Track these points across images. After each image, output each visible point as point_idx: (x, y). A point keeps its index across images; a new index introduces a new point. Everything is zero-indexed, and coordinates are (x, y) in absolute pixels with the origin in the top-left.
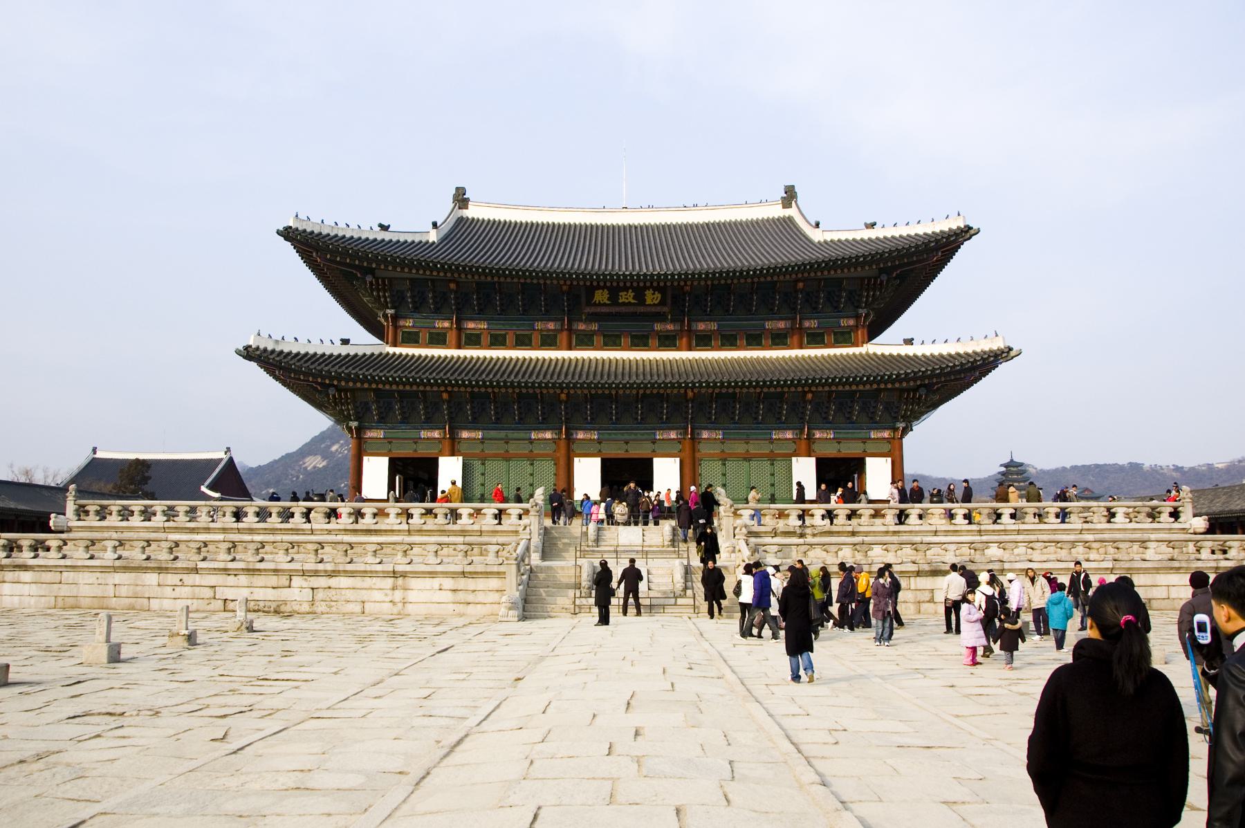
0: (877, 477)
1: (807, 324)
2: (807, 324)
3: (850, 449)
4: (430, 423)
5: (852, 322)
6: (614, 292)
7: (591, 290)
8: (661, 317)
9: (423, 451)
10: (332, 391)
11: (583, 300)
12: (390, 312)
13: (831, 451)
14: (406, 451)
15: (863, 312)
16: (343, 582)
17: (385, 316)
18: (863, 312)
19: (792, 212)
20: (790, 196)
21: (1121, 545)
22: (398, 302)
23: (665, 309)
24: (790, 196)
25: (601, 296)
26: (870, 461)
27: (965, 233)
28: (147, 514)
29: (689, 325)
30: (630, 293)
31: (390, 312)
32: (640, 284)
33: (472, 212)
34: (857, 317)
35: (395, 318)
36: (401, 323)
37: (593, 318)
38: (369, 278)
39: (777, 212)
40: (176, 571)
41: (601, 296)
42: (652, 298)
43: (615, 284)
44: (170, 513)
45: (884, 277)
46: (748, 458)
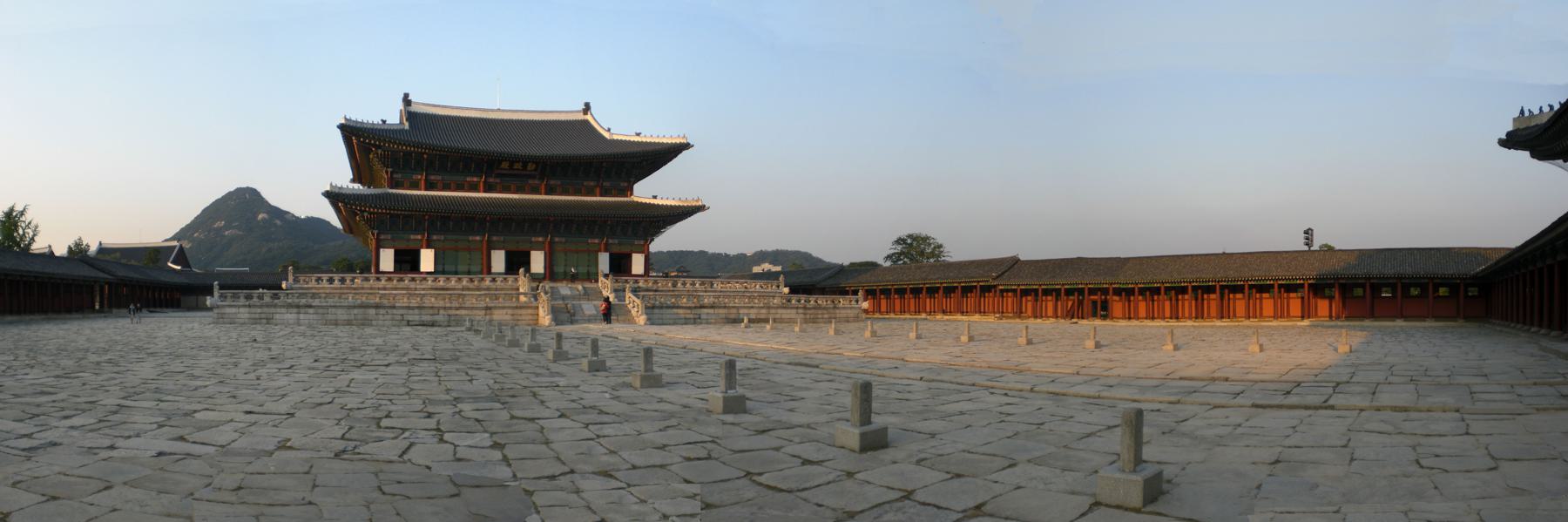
0: (638, 264)
3: (624, 249)
4: (416, 232)
6: (512, 163)
7: (500, 162)
8: (533, 177)
9: (412, 246)
13: (616, 250)
14: (402, 245)
16: (463, 312)
19: (588, 117)
20: (587, 108)
24: (587, 108)
25: (505, 165)
26: (635, 256)
27: (686, 146)
28: (331, 281)
32: (525, 161)
33: (413, 108)
37: (498, 175)
39: (581, 117)
40: (384, 307)
41: (505, 165)
42: (531, 167)
43: (513, 160)
44: (343, 280)
46: (577, 252)
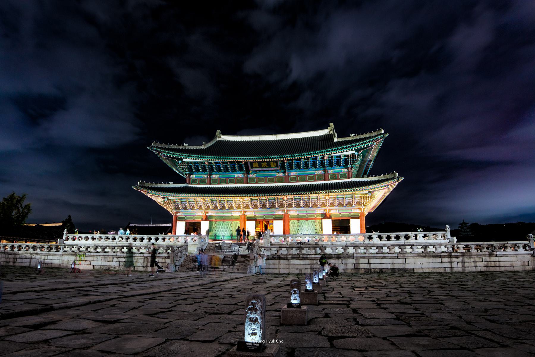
1: (330, 172)
2: (330, 172)
5: (346, 170)
10: (166, 200)
11: (250, 166)
12: (187, 173)
15: (349, 166)
17: (186, 174)
18: (349, 166)
21: (402, 247)
22: (190, 169)
23: (278, 169)
25: (255, 165)
29: (288, 174)
30: (266, 164)
31: (187, 173)
34: (348, 168)
35: (190, 175)
36: (192, 176)
38: (180, 162)
45: (356, 154)
